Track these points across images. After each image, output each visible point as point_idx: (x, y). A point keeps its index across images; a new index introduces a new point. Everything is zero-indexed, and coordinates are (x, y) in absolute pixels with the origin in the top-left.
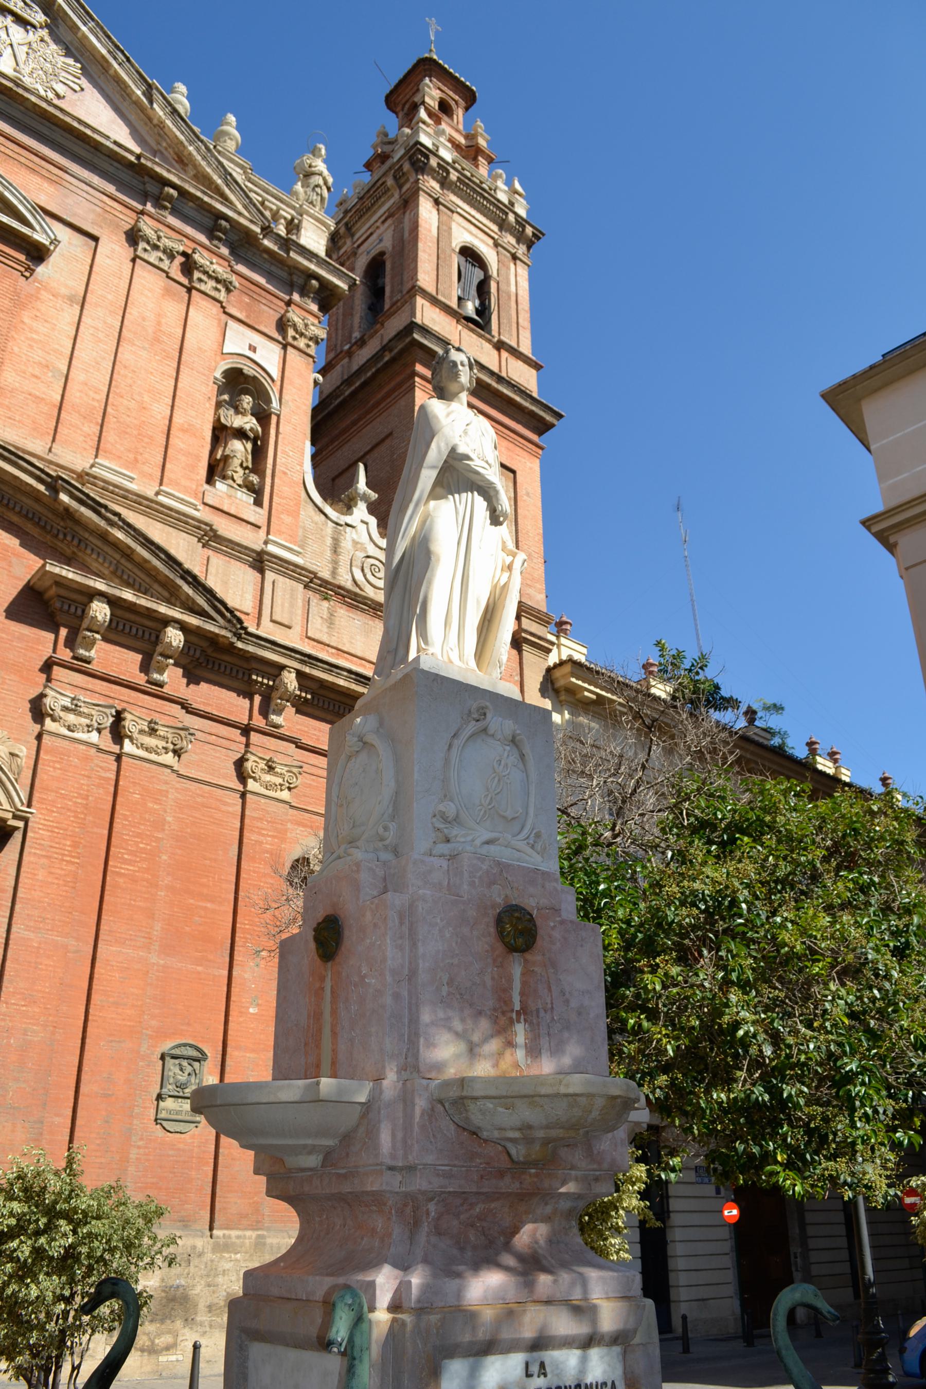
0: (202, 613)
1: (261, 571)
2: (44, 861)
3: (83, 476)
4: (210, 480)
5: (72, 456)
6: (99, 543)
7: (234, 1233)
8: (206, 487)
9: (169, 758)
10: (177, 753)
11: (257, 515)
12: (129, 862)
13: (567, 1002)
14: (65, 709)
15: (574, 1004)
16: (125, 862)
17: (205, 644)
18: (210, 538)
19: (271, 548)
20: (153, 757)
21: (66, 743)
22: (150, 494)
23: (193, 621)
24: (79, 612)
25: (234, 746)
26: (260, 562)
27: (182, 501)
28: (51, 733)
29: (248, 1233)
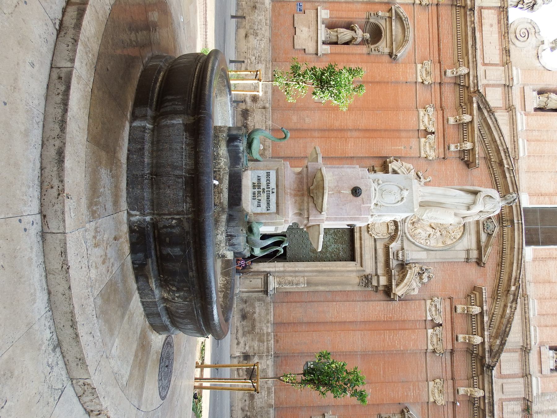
0: (491, 351)
1: (523, 377)
2: (383, 308)
3: (525, 296)
4: (551, 348)
5: (531, 290)
6: (502, 306)
7: (273, 395)
8: (548, 347)
9: (430, 347)
10: (434, 351)
11: (546, 370)
12: (389, 338)
13: (343, 205)
14: (436, 306)
15: (343, 207)
16: (389, 336)
17: (480, 354)
18: (525, 350)
19: (534, 379)
20: (429, 342)
21: (424, 308)
22: (532, 323)
23: (487, 346)
24: (472, 304)
25: (444, 374)
26: (526, 375)
27: (535, 337)
28: (426, 302)
29: (273, 401)
